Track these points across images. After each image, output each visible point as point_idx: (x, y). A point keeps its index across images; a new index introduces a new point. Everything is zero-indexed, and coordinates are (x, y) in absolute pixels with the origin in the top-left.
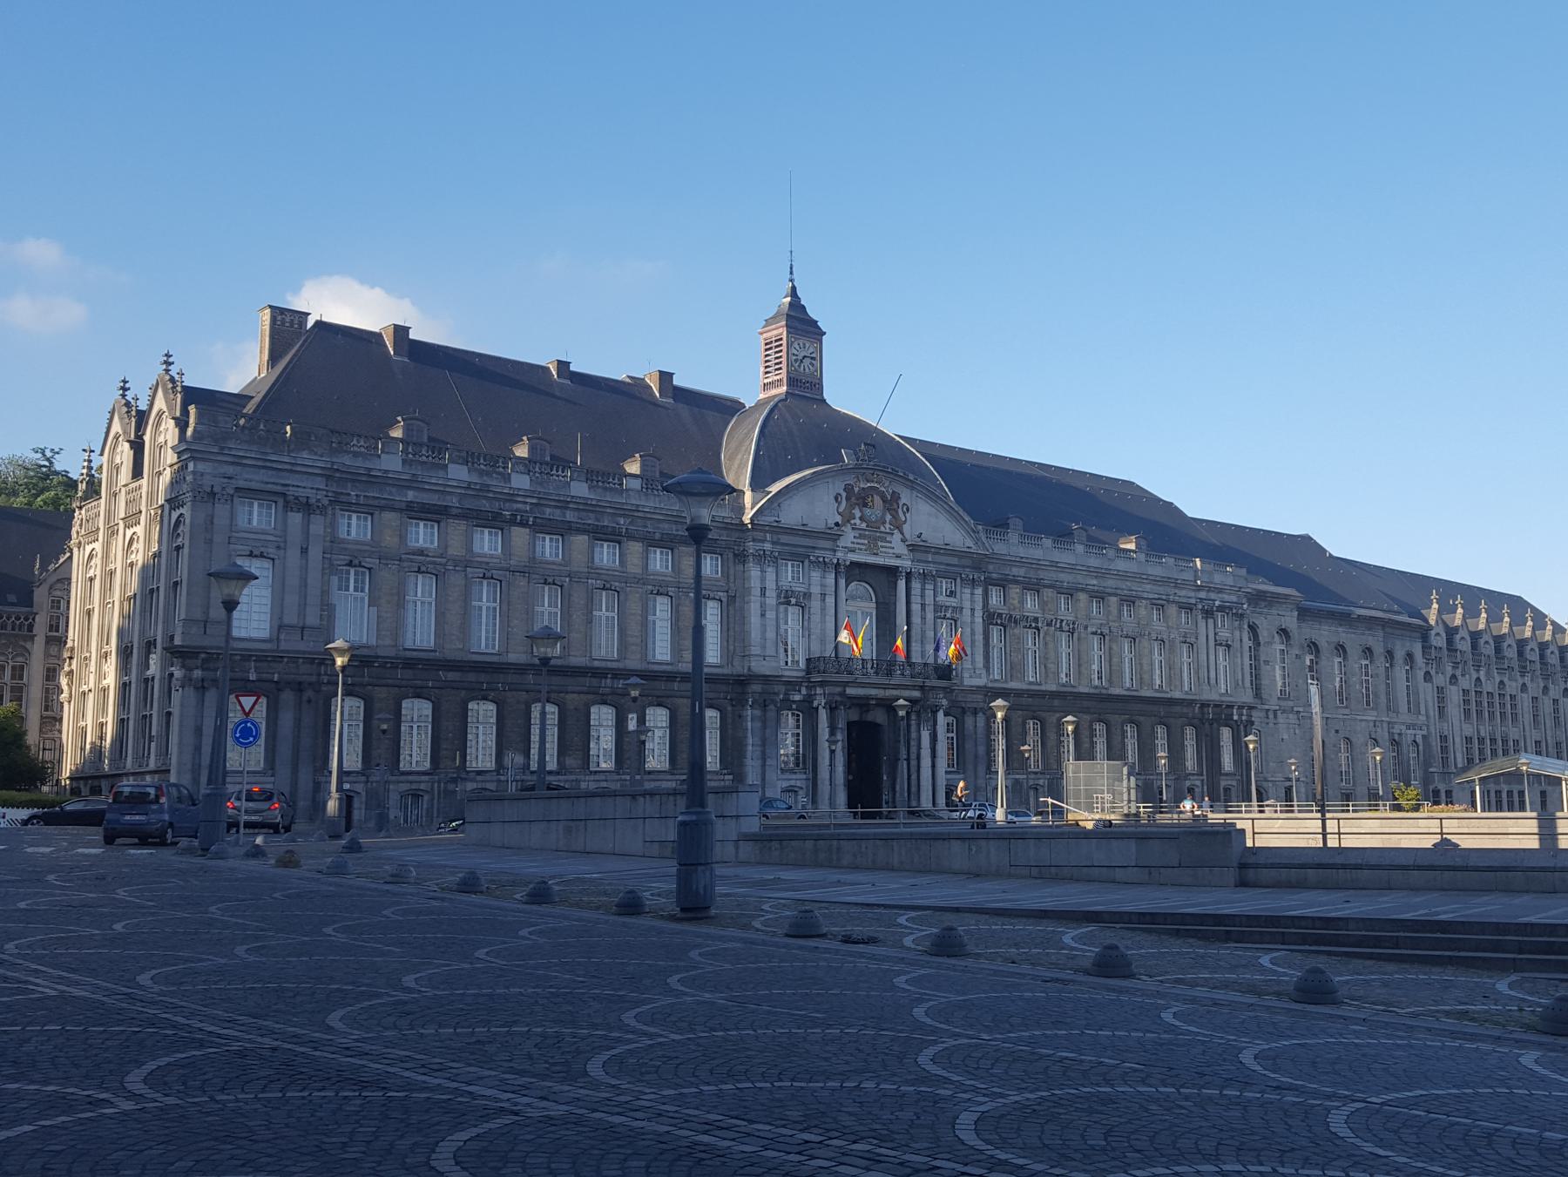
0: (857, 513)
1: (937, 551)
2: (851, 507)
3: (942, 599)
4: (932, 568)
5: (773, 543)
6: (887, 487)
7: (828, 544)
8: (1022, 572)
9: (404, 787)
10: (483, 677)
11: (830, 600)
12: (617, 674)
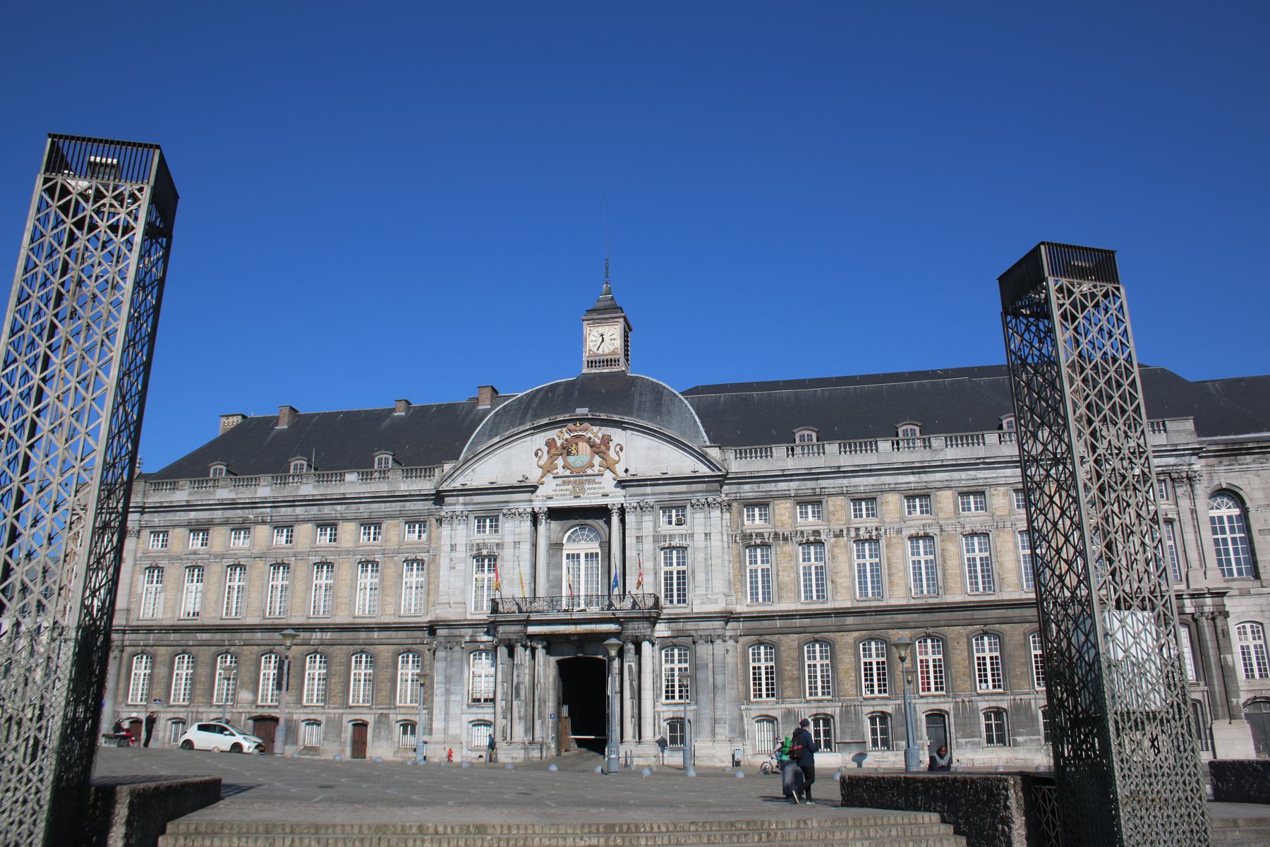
0: (560, 462)
1: (654, 482)
2: (553, 457)
3: (665, 528)
4: (651, 500)
5: (464, 504)
6: (596, 433)
7: (526, 496)
8: (794, 485)
9: (170, 715)
10: (226, 636)
11: (526, 547)
12: (323, 629)
